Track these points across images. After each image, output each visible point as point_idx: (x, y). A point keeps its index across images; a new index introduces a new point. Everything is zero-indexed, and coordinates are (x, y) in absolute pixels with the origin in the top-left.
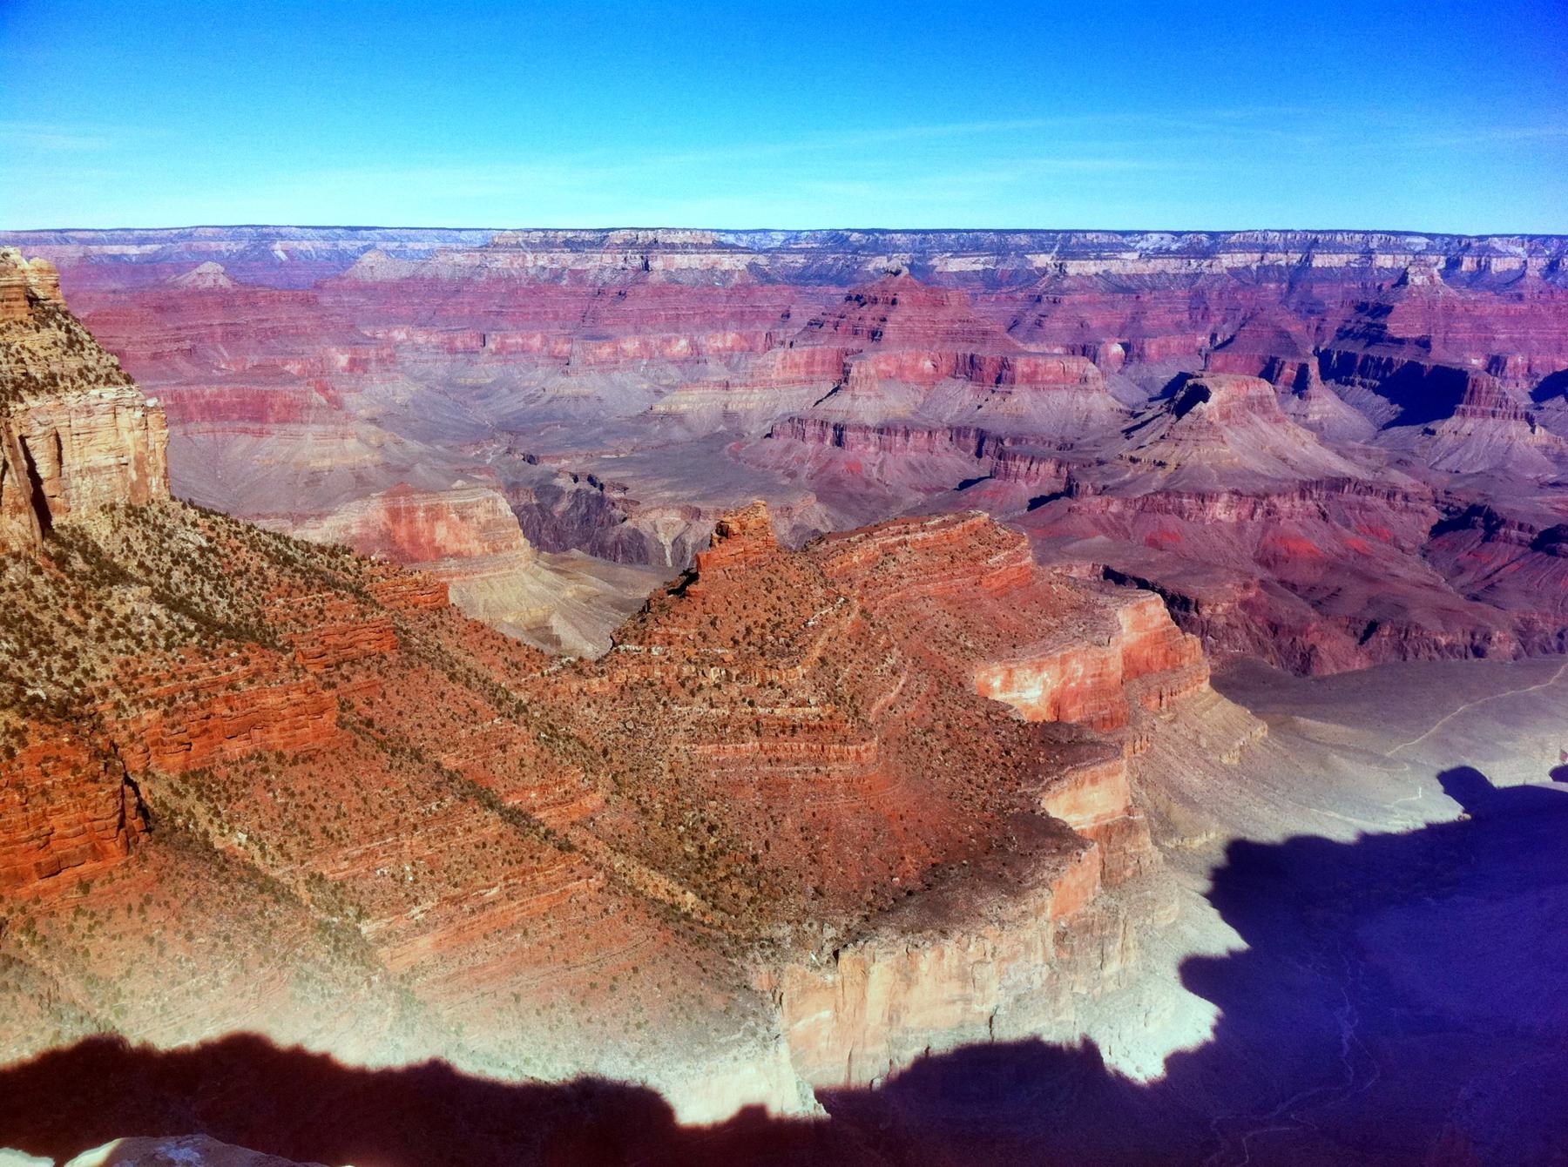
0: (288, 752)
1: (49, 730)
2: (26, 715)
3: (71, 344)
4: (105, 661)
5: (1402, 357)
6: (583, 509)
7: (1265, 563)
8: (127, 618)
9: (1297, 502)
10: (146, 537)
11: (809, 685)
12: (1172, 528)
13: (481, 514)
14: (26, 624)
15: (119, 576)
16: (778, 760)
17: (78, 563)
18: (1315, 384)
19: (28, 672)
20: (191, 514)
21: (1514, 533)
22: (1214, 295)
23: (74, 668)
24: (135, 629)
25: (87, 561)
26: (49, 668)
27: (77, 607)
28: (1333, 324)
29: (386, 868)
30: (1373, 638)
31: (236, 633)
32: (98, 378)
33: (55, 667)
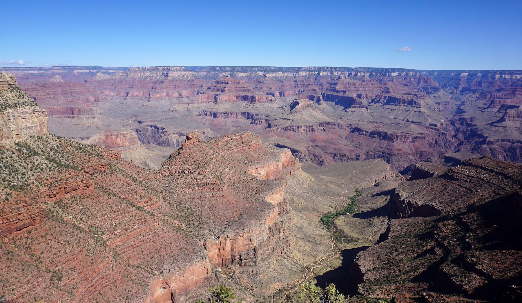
0: (82, 196)
1: (18, 193)
2: (11, 190)
3: (20, 96)
4: (33, 175)
5: (340, 94)
6: (154, 134)
7: (312, 141)
8: (38, 164)
10: (43, 144)
11: (210, 174)
13: (128, 136)
14: (11, 167)
15: (36, 154)
17: (25, 151)
18: (322, 101)
19: (12, 179)
20: (55, 138)
21: (364, 133)
23: (25, 177)
24: (41, 167)
25: (27, 151)
26: (17, 178)
27: (25, 162)
28: (325, 88)
29: (108, 222)
31: (67, 167)
32: (28, 104)
33: (19, 177)
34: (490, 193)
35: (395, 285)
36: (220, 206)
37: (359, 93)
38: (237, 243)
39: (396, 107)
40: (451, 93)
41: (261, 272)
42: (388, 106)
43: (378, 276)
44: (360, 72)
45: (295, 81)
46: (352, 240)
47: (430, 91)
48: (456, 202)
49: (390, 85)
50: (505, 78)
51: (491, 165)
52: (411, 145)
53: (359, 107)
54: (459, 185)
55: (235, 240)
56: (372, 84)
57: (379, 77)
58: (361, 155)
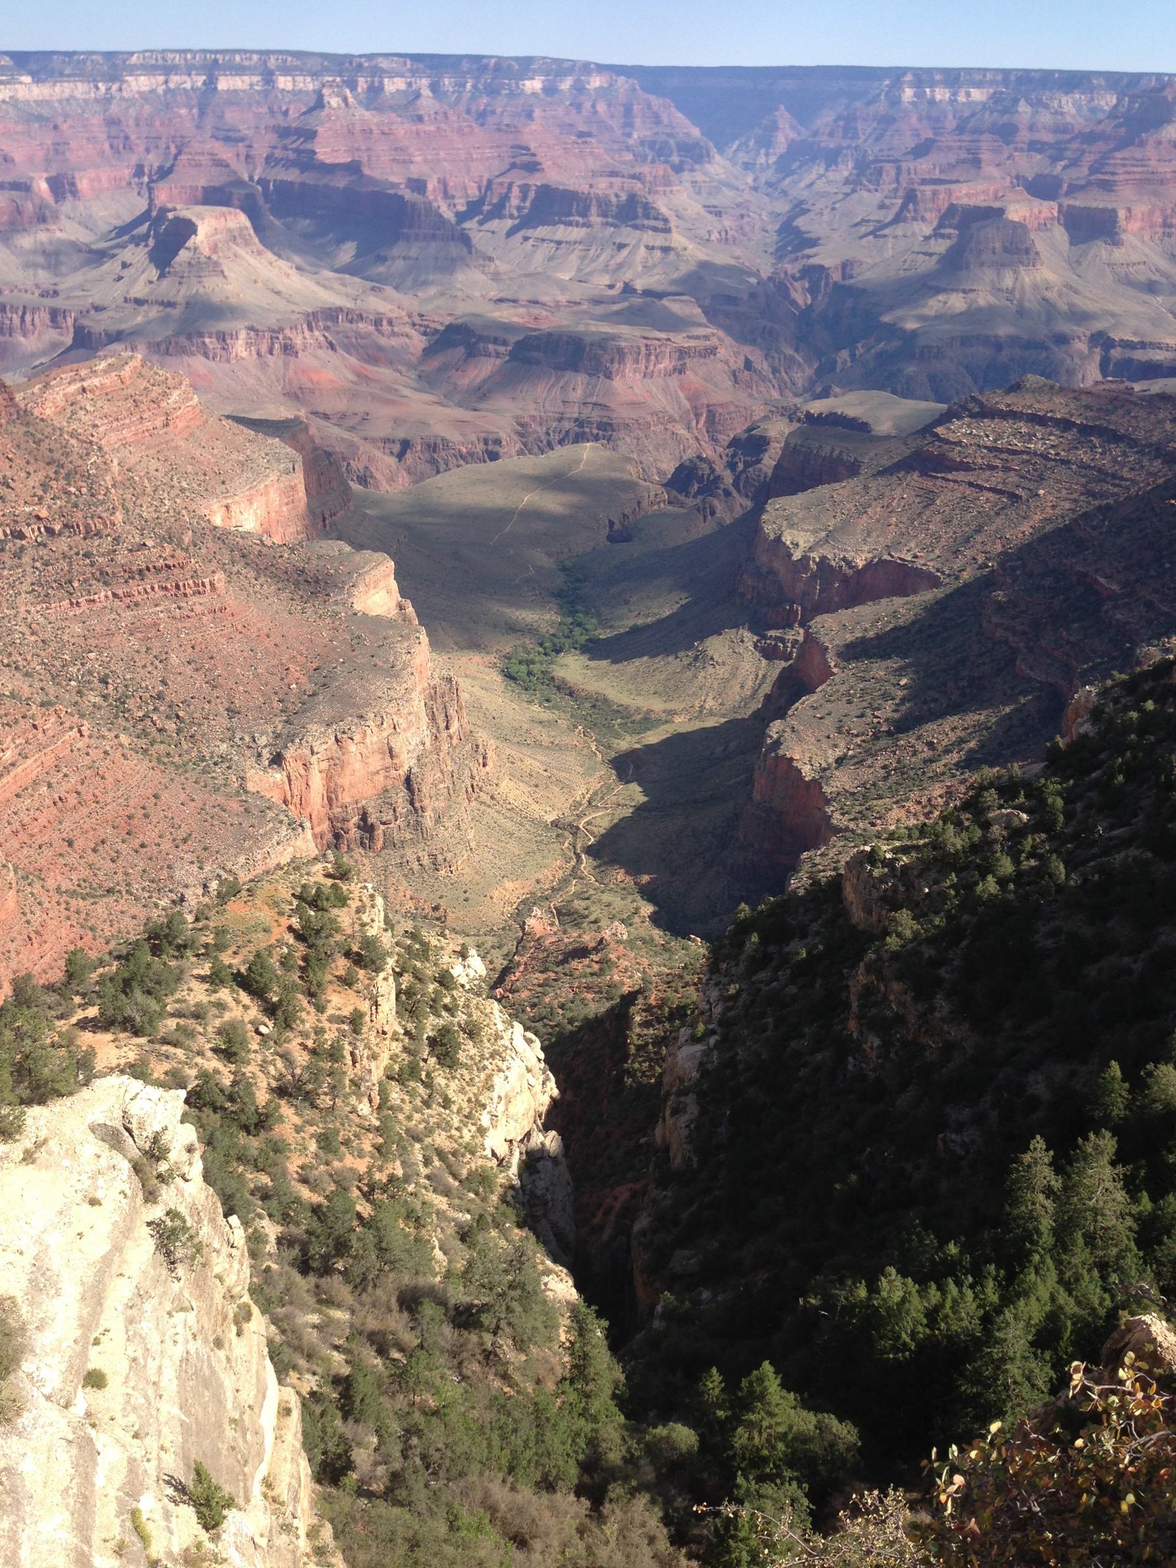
9: (307, 334)
12: (202, 371)
16: (137, 604)
21: (491, 347)
22: (131, 122)
28: (261, 150)
30: (408, 455)
34: (1075, 496)
35: (938, 785)
36: (228, 649)
37: (415, 171)
38: (348, 771)
39: (576, 233)
40: (747, 166)
41: (449, 856)
42: (542, 231)
43: (866, 774)
44: (392, 74)
45: (113, 122)
46: (648, 722)
47: (675, 159)
48: (979, 538)
49: (535, 135)
50: (932, 102)
51: (1059, 407)
52: (674, 382)
53: (434, 237)
54: (971, 484)
55: (336, 764)
56: (460, 130)
57: (473, 98)
58: (503, 436)
